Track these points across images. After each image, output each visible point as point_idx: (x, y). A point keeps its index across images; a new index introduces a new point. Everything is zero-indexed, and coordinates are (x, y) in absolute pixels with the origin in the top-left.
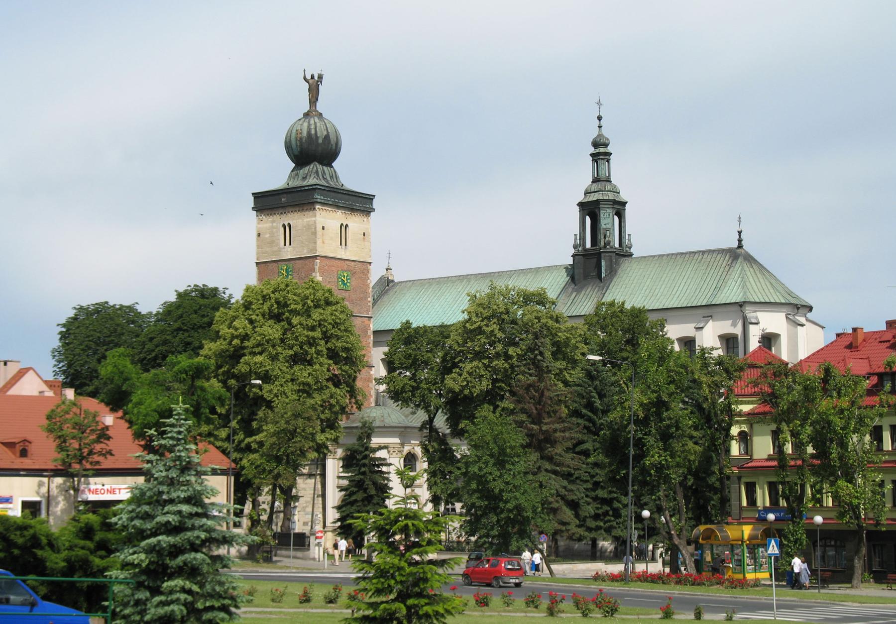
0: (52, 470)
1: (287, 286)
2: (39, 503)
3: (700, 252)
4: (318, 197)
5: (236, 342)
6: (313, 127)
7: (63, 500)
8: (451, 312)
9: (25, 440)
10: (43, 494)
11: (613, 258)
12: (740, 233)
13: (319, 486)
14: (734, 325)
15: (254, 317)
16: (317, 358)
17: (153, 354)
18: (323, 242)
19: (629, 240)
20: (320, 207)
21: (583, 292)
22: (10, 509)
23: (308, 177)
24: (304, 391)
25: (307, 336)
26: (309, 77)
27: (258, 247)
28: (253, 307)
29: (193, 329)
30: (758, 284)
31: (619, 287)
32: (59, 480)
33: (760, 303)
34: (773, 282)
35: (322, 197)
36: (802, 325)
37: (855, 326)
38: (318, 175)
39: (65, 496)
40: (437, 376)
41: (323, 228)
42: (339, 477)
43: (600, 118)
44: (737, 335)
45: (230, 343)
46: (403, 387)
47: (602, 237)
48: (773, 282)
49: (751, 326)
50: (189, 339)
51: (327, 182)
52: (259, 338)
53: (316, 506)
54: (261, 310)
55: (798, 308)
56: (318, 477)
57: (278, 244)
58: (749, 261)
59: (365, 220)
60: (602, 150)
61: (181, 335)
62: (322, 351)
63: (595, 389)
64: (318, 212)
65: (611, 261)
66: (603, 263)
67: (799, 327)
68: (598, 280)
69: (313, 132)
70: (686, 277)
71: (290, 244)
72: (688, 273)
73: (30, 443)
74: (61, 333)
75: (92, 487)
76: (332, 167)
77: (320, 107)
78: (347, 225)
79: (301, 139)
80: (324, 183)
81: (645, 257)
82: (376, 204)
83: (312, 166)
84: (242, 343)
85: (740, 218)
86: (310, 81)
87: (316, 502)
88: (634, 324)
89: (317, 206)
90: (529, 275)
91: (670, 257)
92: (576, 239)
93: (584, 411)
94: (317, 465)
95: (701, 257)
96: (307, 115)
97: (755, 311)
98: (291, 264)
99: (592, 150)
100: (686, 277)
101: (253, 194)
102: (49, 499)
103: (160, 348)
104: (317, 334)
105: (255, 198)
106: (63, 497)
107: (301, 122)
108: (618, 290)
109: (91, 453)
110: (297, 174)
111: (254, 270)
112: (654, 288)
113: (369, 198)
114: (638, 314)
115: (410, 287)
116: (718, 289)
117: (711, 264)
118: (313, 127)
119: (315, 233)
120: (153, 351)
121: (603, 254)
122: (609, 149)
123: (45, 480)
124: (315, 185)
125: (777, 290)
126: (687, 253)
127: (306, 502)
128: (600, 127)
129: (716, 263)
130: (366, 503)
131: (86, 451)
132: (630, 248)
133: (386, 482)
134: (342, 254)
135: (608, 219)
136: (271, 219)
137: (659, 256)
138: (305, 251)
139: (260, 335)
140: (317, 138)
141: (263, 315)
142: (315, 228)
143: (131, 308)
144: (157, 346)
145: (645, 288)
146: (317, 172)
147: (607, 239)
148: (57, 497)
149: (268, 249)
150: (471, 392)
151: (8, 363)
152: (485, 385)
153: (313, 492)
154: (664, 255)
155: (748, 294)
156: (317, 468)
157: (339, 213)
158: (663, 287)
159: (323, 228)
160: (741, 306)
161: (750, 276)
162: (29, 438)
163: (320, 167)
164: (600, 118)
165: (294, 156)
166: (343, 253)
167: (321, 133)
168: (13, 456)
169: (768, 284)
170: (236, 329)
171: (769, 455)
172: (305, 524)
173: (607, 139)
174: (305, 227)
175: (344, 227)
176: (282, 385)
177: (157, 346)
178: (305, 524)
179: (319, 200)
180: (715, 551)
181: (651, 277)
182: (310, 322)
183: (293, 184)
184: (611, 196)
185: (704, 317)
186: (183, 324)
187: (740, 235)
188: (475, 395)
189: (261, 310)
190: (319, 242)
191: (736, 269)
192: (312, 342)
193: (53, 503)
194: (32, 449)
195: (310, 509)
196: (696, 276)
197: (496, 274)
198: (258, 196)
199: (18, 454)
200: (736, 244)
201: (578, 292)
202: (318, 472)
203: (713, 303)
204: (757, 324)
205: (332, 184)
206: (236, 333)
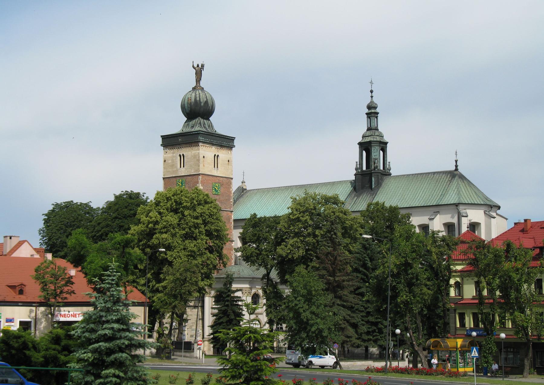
0: (38, 303)
1: (181, 192)
2: (29, 323)
3: (432, 173)
4: (201, 138)
5: (151, 225)
6: (198, 96)
7: (45, 321)
8: (281, 208)
9: (22, 284)
10: (32, 317)
11: (380, 176)
12: (456, 161)
13: (200, 313)
14: (453, 217)
15: (162, 211)
16: (199, 236)
17: (100, 233)
18: (204, 166)
19: (389, 165)
20: (202, 144)
21: (361, 197)
22: (12, 326)
23: (195, 126)
24: (191, 256)
25: (194, 222)
26: (195, 66)
27: (164, 168)
28: (161, 204)
29: (124, 217)
30: (467, 192)
31: (383, 194)
32: (42, 309)
33: (469, 204)
34: (477, 191)
35: (203, 139)
36: (494, 218)
37: (526, 218)
38: (201, 125)
39: (46, 318)
40: (272, 247)
41: (204, 157)
42: (212, 308)
43: (372, 92)
44: (455, 223)
45: (147, 226)
46: (251, 254)
47: (373, 163)
48: (477, 191)
49: (463, 218)
50: (122, 224)
51: (206, 129)
52: (165, 223)
53: (198, 325)
54: (166, 206)
55: (492, 207)
56: (200, 308)
57: (176, 167)
58: (462, 178)
59: (229, 152)
60: (373, 111)
61: (117, 221)
62: (202, 232)
63: (368, 255)
64: (201, 148)
65: (378, 178)
66: (373, 179)
67: (492, 219)
68: (370, 190)
69: (198, 99)
70: (424, 188)
71: (184, 167)
72: (425, 186)
73: (25, 286)
74: (44, 219)
75: (62, 313)
76: (210, 120)
77: (202, 84)
78: (218, 156)
79: (191, 103)
80: (204, 130)
81: (398, 176)
82: (236, 142)
83: (197, 120)
84: (154, 226)
85: (456, 152)
86: (197, 68)
87: (198, 323)
88: (392, 216)
89: (200, 144)
90: (328, 186)
91: (414, 175)
92: (357, 165)
93: (361, 269)
94: (199, 300)
95: (432, 176)
96: (194, 89)
97: (465, 209)
98: (184, 179)
99: (367, 111)
100: (424, 188)
101: (161, 136)
102: (36, 320)
103: (103, 230)
104: (200, 221)
105: (162, 139)
106: (44, 319)
107: (191, 93)
108: (382, 196)
109: (61, 292)
110: (188, 125)
111: (162, 182)
112: (404, 194)
113: (232, 139)
114: (394, 210)
115: (257, 193)
116: (443, 195)
117: (439, 180)
118: (198, 96)
119: (199, 160)
120: (100, 231)
121: (373, 174)
122: (378, 110)
123: (34, 308)
124: (199, 131)
125: (479, 196)
126: (424, 174)
127: (192, 323)
128: (372, 97)
129: (442, 180)
130: (228, 323)
131: (58, 291)
132: (390, 170)
133: (241, 311)
134: (215, 173)
135: (377, 153)
136: (172, 151)
137: (407, 175)
138: (193, 171)
139: (165, 221)
140: (200, 102)
141: (167, 209)
142: (199, 157)
143: (87, 205)
144: (102, 228)
145: (399, 194)
146: (200, 123)
147: (376, 165)
148: (41, 319)
149: (170, 170)
150: (293, 257)
151: (12, 238)
152: (301, 252)
153: (196, 317)
154: (410, 175)
155: (462, 199)
156: (199, 303)
157: (214, 148)
158: (410, 194)
159: (204, 157)
160: (457, 206)
161: (463, 188)
162: (25, 283)
163: (202, 120)
164: (372, 92)
165: (186, 113)
166: (216, 172)
167: (203, 100)
168: (15, 294)
169: (473, 192)
170: (151, 218)
171: (473, 296)
172: (192, 336)
173: (376, 104)
174: (192, 156)
175: (216, 157)
176: (178, 252)
177: (102, 228)
178: (192, 336)
179: (201, 140)
180: (440, 355)
181: (402, 188)
182: (195, 214)
183: (185, 131)
184: (378, 139)
185: (434, 212)
186: (118, 214)
187: (456, 163)
188: (295, 258)
189: (166, 206)
190: (201, 165)
191: (454, 183)
192: (196, 226)
193: (38, 323)
194: (26, 289)
195: (194, 327)
196: (430, 187)
197: (308, 186)
198: (164, 138)
199: (18, 293)
200: (454, 168)
201: (358, 197)
202: (200, 305)
203: (440, 204)
204: (467, 216)
205: (209, 130)
206: (151, 220)
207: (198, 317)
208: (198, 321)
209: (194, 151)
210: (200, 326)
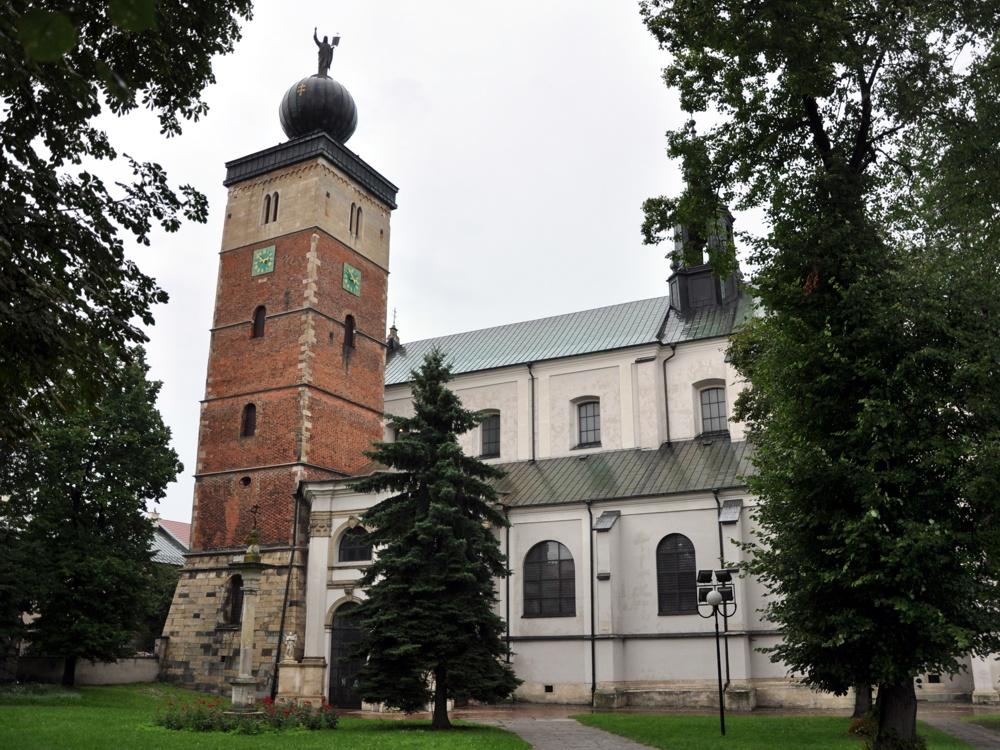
13: (294, 587)
18: (327, 215)
26: (321, 40)
82: (399, 199)
87: (287, 614)
89: (321, 161)
127: (270, 615)
134: (350, 241)
138: (298, 224)
153: (283, 597)
159: (328, 195)
207: (289, 597)
208: (288, 609)
209: (305, 179)
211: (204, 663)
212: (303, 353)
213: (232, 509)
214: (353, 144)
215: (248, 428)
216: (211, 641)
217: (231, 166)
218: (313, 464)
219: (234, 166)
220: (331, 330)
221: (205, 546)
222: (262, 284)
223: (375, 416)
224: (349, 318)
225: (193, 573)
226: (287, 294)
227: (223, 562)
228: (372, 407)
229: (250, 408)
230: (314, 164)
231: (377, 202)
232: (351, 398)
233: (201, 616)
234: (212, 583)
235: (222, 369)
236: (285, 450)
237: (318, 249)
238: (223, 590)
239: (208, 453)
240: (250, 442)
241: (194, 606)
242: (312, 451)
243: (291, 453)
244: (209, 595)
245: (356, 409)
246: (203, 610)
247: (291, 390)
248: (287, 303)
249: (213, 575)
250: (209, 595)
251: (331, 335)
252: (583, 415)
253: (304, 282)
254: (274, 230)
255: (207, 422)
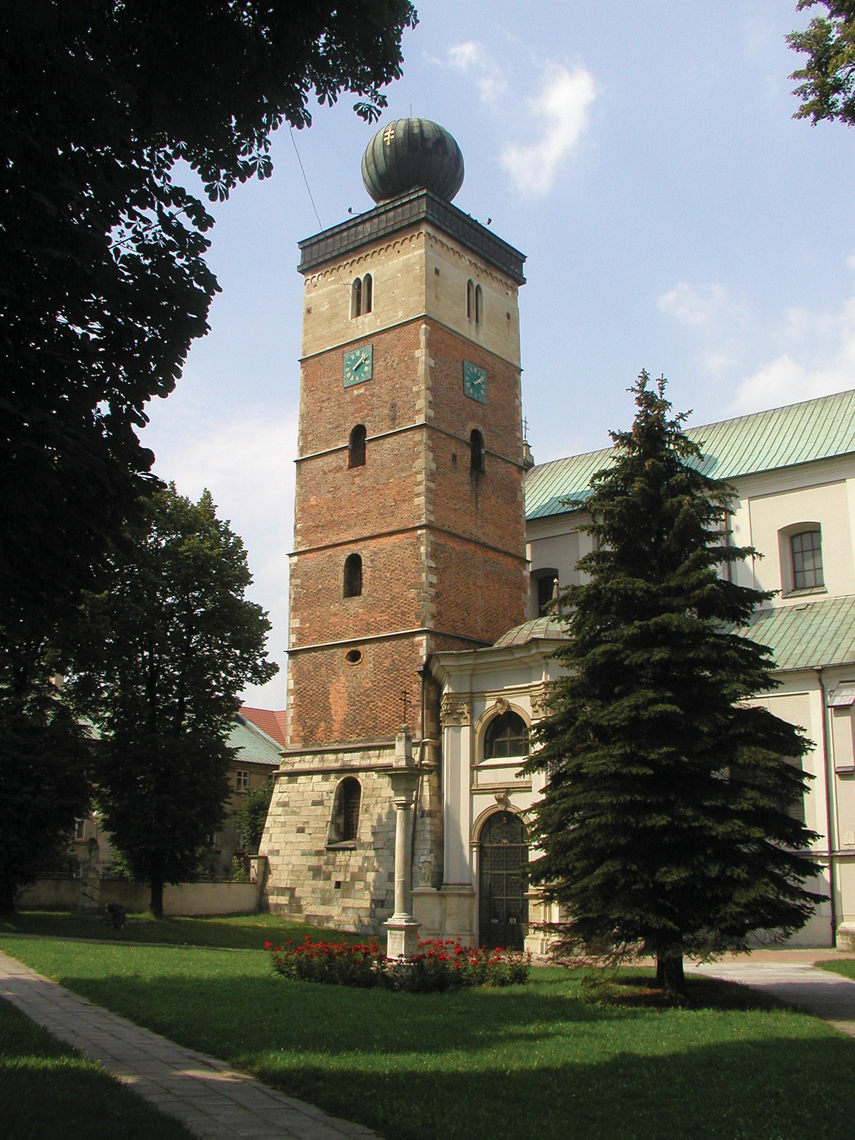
18: (437, 298)
69: (416, 131)
87: (418, 828)
111: (298, 373)
138: (400, 314)
165: (377, 172)
166: (473, 332)
208: (419, 821)
210: (425, 840)
211: (313, 891)
212: (420, 483)
213: (339, 692)
214: (462, 201)
215: (353, 586)
216: (322, 862)
217: (306, 245)
218: (443, 630)
219: (312, 245)
220: (454, 451)
221: (306, 740)
222: (357, 395)
223: (516, 562)
224: (476, 434)
225: (293, 775)
226: (393, 406)
227: (331, 761)
228: (512, 551)
229: (354, 563)
230: (416, 234)
231: (499, 277)
232: (484, 539)
233: (307, 831)
234: (317, 788)
235: (313, 511)
236: (403, 613)
237: (429, 345)
238: (333, 796)
239: (303, 621)
240: (355, 604)
241: (297, 818)
242: (439, 613)
243: (412, 617)
244: (315, 803)
245: (491, 554)
246: (307, 823)
247: (407, 535)
248: (393, 419)
249: (318, 778)
250: (315, 803)
251: (454, 457)
252: (797, 548)
253: (415, 389)
254: (367, 324)
255: (298, 581)
